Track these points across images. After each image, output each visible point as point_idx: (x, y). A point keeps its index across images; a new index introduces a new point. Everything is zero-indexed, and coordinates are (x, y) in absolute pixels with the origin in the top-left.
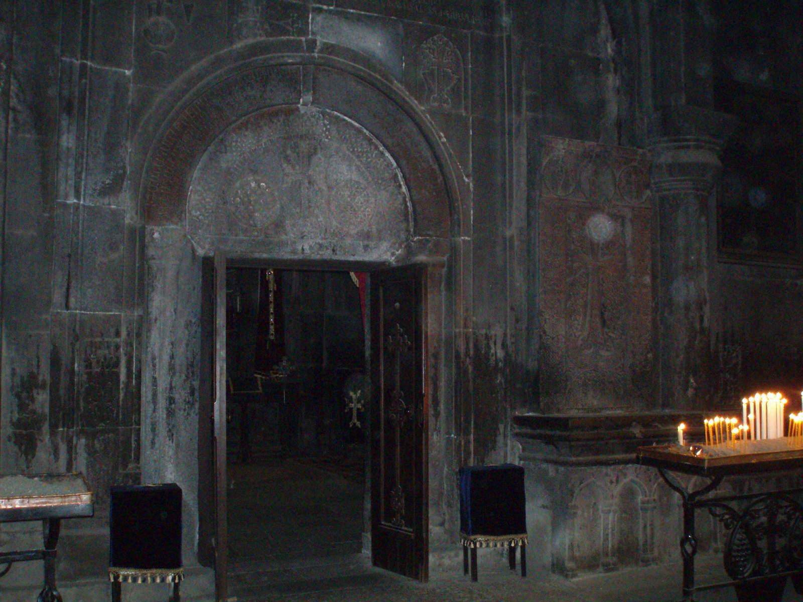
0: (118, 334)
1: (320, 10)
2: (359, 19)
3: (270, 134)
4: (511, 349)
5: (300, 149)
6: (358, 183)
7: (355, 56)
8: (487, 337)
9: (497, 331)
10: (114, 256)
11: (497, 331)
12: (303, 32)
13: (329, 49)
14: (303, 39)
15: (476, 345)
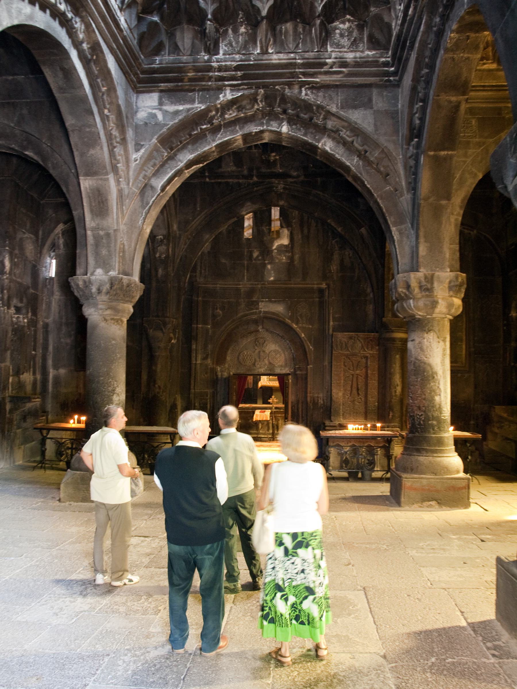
0: (207, 396)
1: (263, 301)
2: (275, 302)
3: (251, 338)
4: (325, 401)
5: (259, 343)
6: (278, 351)
7: (273, 313)
8: (318, 397)
9: (321, 395)
10: (206, 376)
11: (321, 395)
12: (257, 309)
13: (265, 312)
14: (257, 311)
15: (314, 400)
